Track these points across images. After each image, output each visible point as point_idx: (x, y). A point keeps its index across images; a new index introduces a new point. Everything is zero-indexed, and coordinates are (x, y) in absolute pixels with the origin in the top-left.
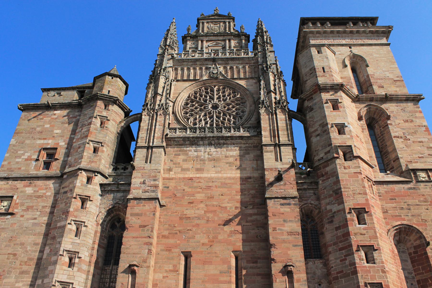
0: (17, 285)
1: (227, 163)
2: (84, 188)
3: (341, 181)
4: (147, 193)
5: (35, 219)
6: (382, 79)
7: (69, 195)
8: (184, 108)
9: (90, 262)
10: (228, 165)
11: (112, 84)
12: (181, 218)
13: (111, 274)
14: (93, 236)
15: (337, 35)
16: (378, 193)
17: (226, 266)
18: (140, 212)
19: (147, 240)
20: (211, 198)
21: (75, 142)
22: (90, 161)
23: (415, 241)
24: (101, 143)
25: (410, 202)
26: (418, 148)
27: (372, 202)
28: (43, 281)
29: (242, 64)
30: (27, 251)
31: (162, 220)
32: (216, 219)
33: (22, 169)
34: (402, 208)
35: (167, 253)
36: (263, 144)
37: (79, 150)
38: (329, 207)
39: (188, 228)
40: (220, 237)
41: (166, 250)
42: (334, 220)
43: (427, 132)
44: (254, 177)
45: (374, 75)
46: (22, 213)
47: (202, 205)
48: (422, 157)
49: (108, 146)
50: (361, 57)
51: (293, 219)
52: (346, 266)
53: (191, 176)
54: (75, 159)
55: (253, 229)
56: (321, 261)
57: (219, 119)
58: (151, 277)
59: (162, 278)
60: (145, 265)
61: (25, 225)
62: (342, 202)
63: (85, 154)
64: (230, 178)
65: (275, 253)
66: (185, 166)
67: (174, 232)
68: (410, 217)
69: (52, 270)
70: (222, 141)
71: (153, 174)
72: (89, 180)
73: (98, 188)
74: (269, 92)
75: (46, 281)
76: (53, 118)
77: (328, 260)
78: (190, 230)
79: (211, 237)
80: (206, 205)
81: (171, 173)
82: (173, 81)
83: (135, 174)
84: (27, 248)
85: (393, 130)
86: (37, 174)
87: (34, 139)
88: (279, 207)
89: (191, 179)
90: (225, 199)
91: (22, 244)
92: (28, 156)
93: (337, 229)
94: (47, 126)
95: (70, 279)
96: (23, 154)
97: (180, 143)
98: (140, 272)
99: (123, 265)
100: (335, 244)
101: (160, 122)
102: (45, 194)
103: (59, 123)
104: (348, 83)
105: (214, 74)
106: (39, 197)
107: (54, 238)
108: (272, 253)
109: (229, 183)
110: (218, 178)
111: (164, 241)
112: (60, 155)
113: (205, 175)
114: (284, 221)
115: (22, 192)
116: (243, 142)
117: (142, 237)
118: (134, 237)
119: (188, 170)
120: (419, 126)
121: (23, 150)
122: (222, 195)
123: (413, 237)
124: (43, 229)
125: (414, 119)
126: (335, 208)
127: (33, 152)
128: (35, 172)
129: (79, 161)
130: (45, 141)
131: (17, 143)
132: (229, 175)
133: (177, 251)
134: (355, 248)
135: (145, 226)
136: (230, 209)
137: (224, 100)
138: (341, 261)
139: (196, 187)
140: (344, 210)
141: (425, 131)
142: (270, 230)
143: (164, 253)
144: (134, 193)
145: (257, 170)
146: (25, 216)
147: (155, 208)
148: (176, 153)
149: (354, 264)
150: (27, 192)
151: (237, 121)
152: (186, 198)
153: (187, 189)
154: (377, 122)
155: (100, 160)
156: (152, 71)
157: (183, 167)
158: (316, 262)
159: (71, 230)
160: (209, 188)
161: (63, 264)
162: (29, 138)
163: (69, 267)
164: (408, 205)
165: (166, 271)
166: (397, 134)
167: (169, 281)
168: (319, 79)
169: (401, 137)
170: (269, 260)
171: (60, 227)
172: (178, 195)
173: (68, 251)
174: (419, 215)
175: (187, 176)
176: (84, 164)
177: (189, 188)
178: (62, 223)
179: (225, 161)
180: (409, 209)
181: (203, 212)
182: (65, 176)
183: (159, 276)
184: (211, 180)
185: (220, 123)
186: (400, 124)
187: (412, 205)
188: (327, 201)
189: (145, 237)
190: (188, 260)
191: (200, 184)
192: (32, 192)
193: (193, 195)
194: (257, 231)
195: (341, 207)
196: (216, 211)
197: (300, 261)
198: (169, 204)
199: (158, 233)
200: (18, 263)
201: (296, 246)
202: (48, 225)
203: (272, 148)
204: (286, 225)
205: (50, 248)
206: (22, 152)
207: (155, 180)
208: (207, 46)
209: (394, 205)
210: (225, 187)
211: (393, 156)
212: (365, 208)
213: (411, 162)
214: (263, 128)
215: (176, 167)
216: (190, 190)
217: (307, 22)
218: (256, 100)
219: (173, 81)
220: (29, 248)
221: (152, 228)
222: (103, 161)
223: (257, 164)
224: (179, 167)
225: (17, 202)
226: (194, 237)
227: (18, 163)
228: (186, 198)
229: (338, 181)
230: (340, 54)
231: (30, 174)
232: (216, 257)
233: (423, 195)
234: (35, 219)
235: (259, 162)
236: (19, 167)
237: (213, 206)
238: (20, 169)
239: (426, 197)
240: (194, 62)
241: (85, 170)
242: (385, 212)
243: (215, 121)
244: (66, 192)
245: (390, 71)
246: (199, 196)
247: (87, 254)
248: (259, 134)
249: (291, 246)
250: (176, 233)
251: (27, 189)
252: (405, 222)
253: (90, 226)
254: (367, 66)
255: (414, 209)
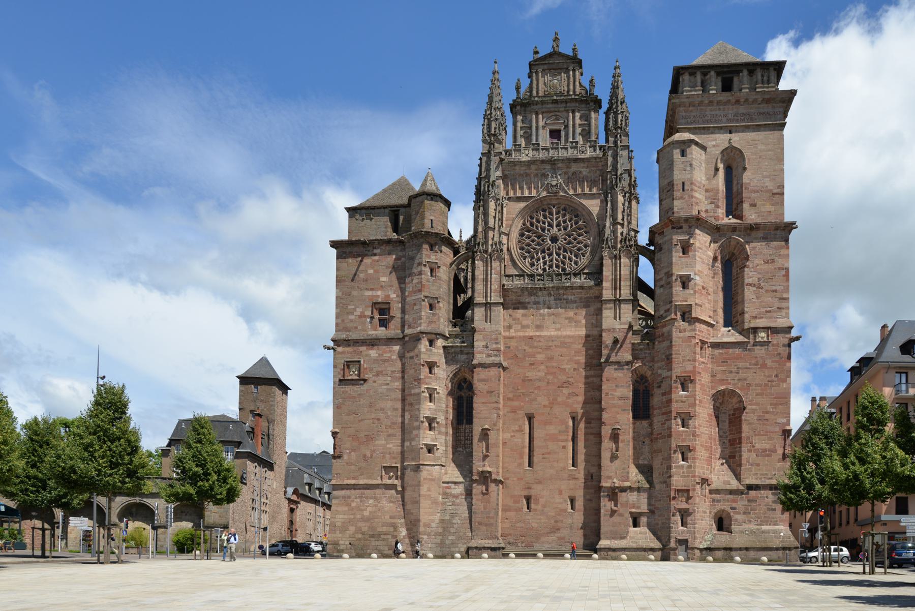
0: (388, 446)
1: (567, 319)
2: (429, 353)
3: (673, 347)
4: (491, 358)
5: (388, 384)
6: (758, 191)
7: (416, 360)
8: (519, 242)
9: (446, 425)
10: (567, 321)
11: (433, 208)
12: (523, 381)
13: (465, 433)
14: (445, 400)
15: (718, 107)
16: (712, 355)
17: (564, 426)
18: (486, 378)
19: (495, 405)
20: (551, 359)
21: (408, 296)
22: (429, 322)
23: (736, 404)
24: (437, 298)
25: (741, 365)
26: (768, 299)
27: (699, 367)
28: (411, 443)
29: (587, 167)
30: (388, 416)
31: (506, 382)
32: (556, 380)
33: (359, 328)
34: (731, 372)
35: (513, 414)
36: (603, 299)
37: (416, 308)
38: (660, 371)
39: (531, 391)
40: (559, 399)
41: (512, 412)
42: (662, 385)
43: (785, 278)
44: (592, 336)
45: (749, 183)
46: (373, 379)
47: (543, 367)
48: (770, 311)
49: (444, 300)
50: (740, 151)
51: (625, 384)
52: (664, 430)
53: (531, 334)
54: (413, 318)
55: (590, 391)
56: (648, 421)
57: (559, 257)
58: (501, 438)
59: (509, 437)
60: (495, 428)
61: (380, 391)
62: (671, 370)
63: (423, 313)
64: (569, 337)
65: (605, 416)
66: (525, 323)
67: (518, 394)
68: (736, 381)
69: (417, 435)
70: (561, 292)
71: (494, 337)
72: (431, 343)
73: (441, 351)
74: (615, 223)
75: (413, 443)
76: (374, 261)
77: (653, 421)
78: (532, 392)
79: (551, 399)
80: (547, 367)
81: (511, 331)
82: (504, 199)
83: (476, 336)
84: (387, 413)
85: (748, 274)
86: (376, 335)
87: (361, 290)
88: (613, 372)
89: (531, 338)
90: (564, 360)
91: (382, 409)
92: (361, 312)
93: (663, 394)
94: (371, 271)
95: (433, 441)
96: (355, 310)
97: (519, 294)
98: (492, 435)
99: (477, 429)
100: (659, 408)
101: (495, 269)
102: (390, 357)
103: (383, 267)
104: (714, 199)
105: (553, 186)
106: (385, 361)
107: (411, 405)
108: (603, 417)
109: (568, 343)
110: (558, 337)
111: (510, 403)
112: (396, 311)
113: (545, 333)
114: (616, 386)
115: (367, 355)
116: (584, 292)
117: (490, 403)
118: (483, 403)
119: (527, 327)
120: (779, 269)
121: (353, 305)
122: (561, 356)
123: (735, 400)
124: (399, 395)
125: (776, 259)
126: (665, 374)
127: (364, 306)
128: (373, 332)
129: (419, 322)
130: (374, 293)
131: (343, 294)
132: (568, 333)
133: (521, 413)
134: (674, 414)
135: (492, 392)
136: (569, 370)
137: (565, 229)
138: (662, 424)
139: (536, 347)
140: (671, 377)
141: (784, 276)
142: (603, 396)
143: (511, 414)
144: (479, 358)
145: (597, 327)
146: (378, 382)
147: (500, 373)
148: (515, 306)
149: (671, 428)
150: (372, 356)
151: (579, 260)
152: (527, 359)
153: (529, 350)
154: (736, 259)
155: (439, 319)
156: (477, 178)
157: (523, 324)
158: (643, 422)
159: (426, 397)
160: (548, 348)
161: (425, 429)
162: (354, 287)
163: (430, 430)
164: (738, 368)
165: (513, 431)
166: (750, 281)
167: (516, 440)
168: (676, 203)
169: (755, 285)
170: (600, 422)
171: (414, 394)
172: (520, 356)
173: (427, 418)
174: (745, 379)
175: (527, 335)
176: (423, 327)
177: (530, 347)
178: (417, 391)
179: (564, 316)
180: (738, 373)
181: (544, 374)
182: (407, 339)
183: (508, 435)
184: (550, 338)
185: (560, 263)
186: (758, 265)
187: (741, 368)
188: (659, 364)
189: (493, 403)
190: (532, 420)
191: (540, 344)
192: (377, 355)
193: (534, 356)
194: (593, 393)
195: (669, 374)
196: (555, 373)
197: (626, 424)
198: (512, 366)
199: (504, 396)
200: (383, 427)
201: (624, 410)
202: (403, 390)
203: (612, 305)
204: (618, 390)
205: (410, 413)
206: (353, 307)
207: (497, 343)
208: (544, 124)
209: (724, 368)
210: (565, 347)
211: (739, 308)
212: (690, 376)
213: (756, 317)
214: (604, 278)
215: (516, 324)
216: (530, 350)
217: (683, 72)
218: (601, 230)
219: (504, 199)
220: (389, 413)
221: (499, 394)
222: (442, 320)
223: (597, 319)
224: (518, 324)
225: (365, 366)
226: (535, 400)
227: (351, 321)
228: (527, 359)
229: (670, 347)
230: (714, 146)
231: (370, 335)
232: (556, 418)
233: (756, 357)
234: (388, 384)
235: (599, 317)
236: (355, 325)
237: (553, 367)
238: (356, 328)
239: (759, 359)
240: (527, 165)
241: (426, 333)
242: (713, 376)
243: (554, 261)
244: (412, 358)
245: (771, 177)
246: (540, 357)
247: (443, 418)
248: (599, 283)
249: (620, 410)
250: (520, 396)
251: (370, 351)
252: (730, 387)
253: (441, 392)
254: (745, 169)
255: (743, 373)
